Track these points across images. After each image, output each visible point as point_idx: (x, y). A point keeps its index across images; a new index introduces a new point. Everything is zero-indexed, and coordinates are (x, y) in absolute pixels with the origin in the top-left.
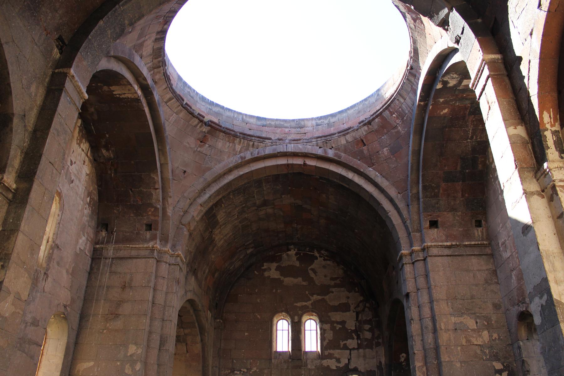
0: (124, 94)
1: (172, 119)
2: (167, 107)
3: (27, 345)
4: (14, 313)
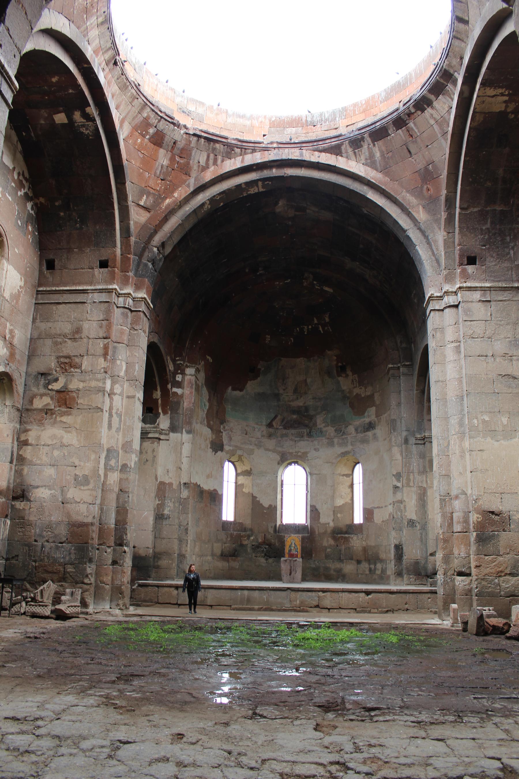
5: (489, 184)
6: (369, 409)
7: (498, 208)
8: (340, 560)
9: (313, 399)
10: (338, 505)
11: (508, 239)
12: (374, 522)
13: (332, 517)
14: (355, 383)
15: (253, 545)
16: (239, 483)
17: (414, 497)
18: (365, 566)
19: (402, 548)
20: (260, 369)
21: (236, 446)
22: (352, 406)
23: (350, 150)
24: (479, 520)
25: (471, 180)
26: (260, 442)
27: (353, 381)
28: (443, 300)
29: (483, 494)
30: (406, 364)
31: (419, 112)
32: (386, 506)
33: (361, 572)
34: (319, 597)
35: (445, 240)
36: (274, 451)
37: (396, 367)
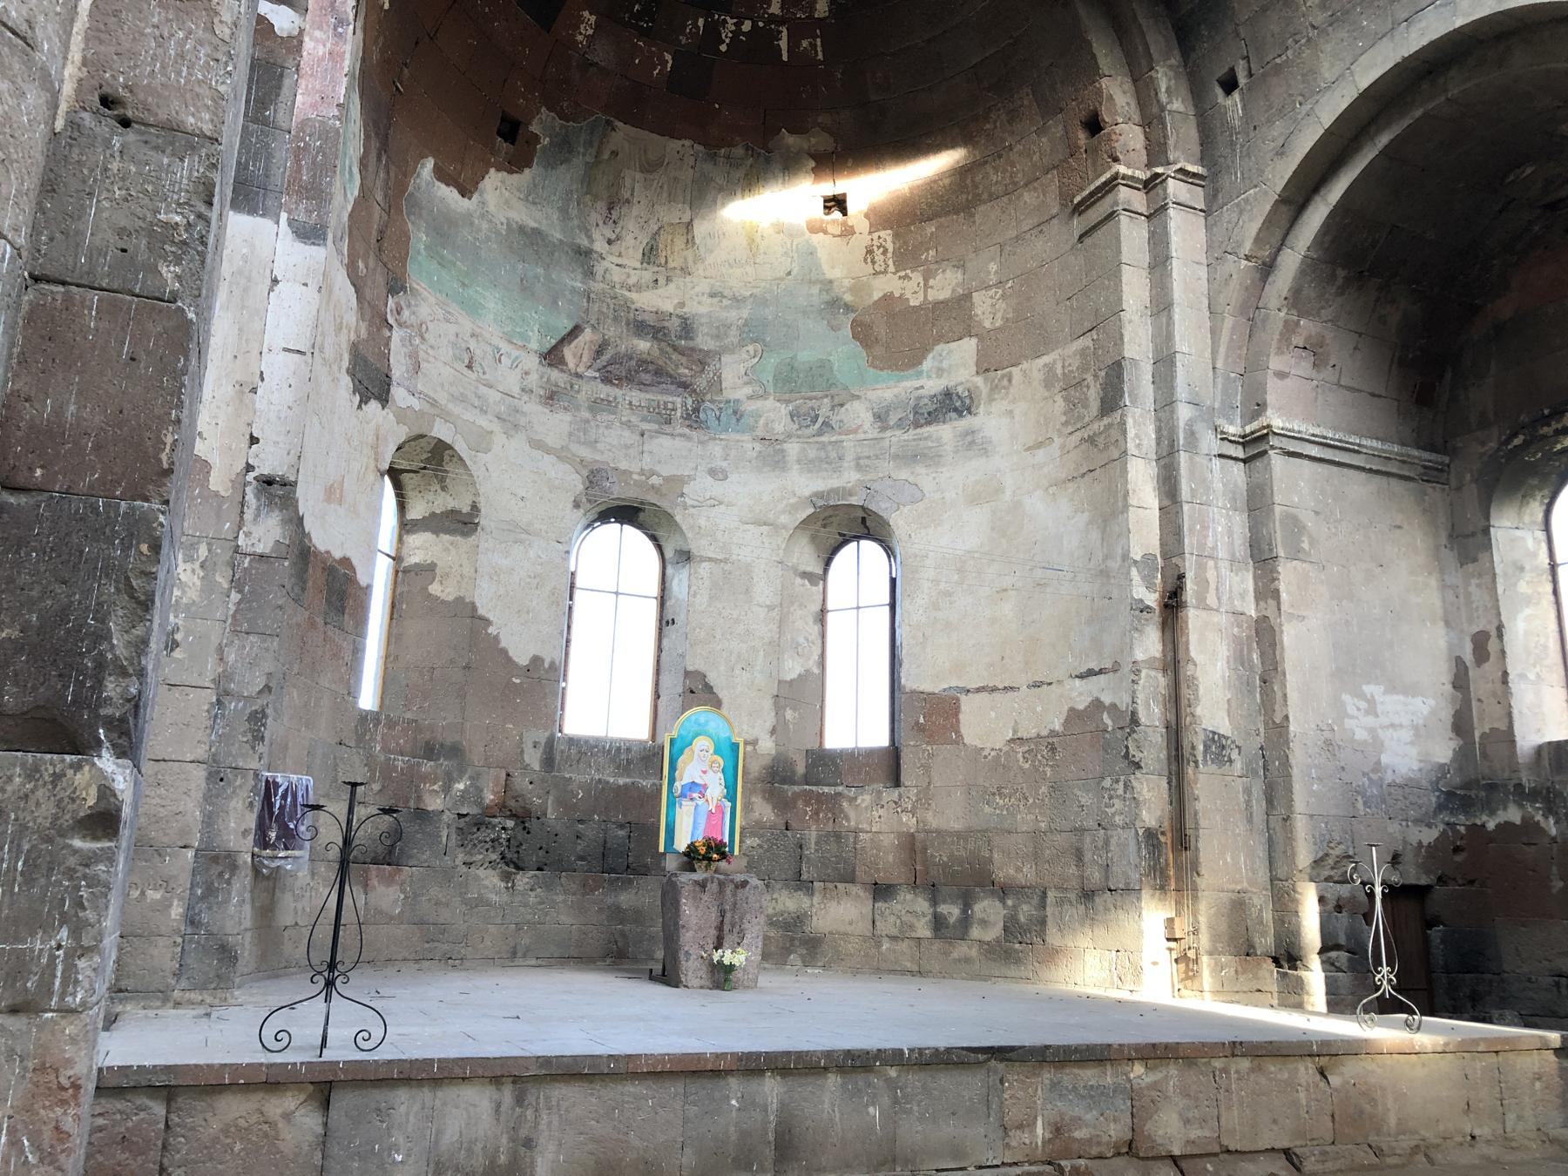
6: (938, 348)
8: (799, 883)
9: (712, 295)
10: (788, 679)
12: (959, 740)
13: (770, 720)
14: (879, 257)
15: (460, 816)
16: (413, 558)
17: (1223, 651)
18: (913, 908)
20: (536, 138)
21: (434, 403)
22: (863, 333)
26: (517, 411)
27: (870, 252)
32: (1037, 685)
33: (895, 932)
34: (1133, 1094)
36: (561, 455)
37: (1137, 180)
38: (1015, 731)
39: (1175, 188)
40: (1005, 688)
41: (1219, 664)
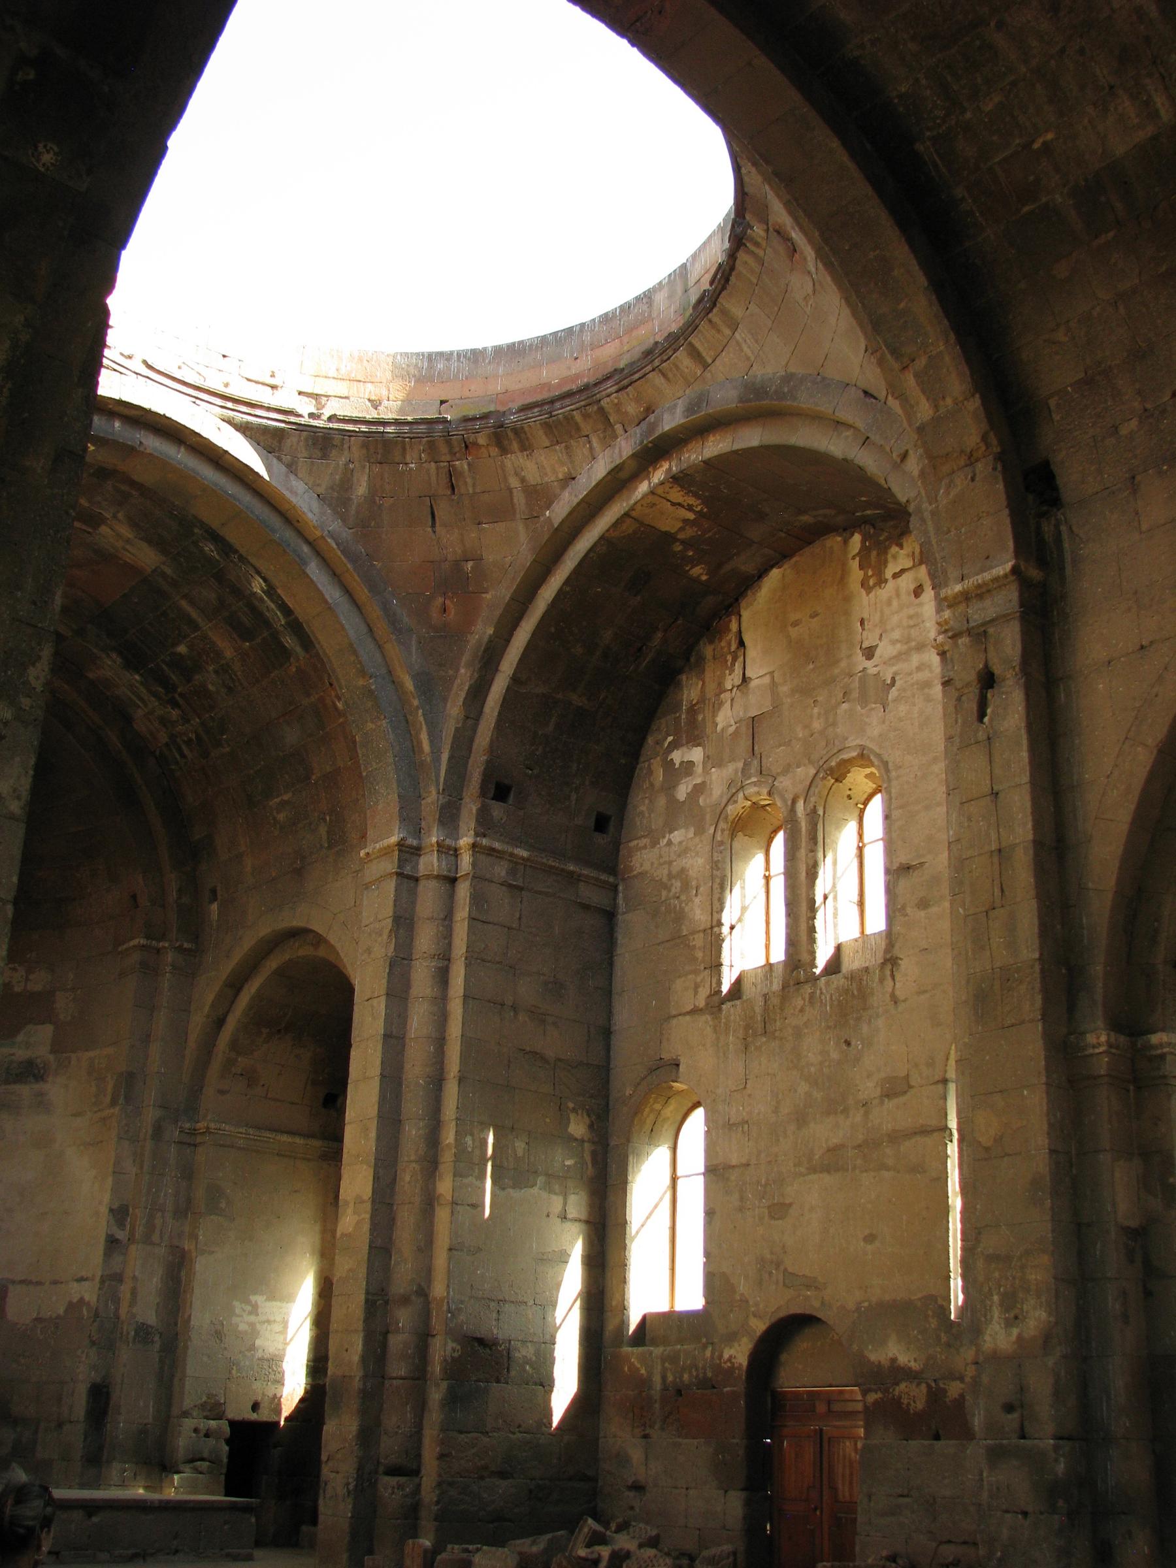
0: (673, 504)
1: (749, 347)
2: (717, 362)
3: (888, 1151)
4: (358, 1223)
5: (578, 650)
6: (29, 1027)
7: (577, 700)
11: (574, 767)
19: (108, 1393)
23: (303, 453)
24: (456, 1355)
25: (553, 630)
28: (420, 855)
29: (467, 1299)
30: (186, 945)
31: (494, 451)
32: (55, 1282)
35: (457, 729)
38: (38, 1313)
39: (170, 957)
40: (37, 1282)
41: (155, 1280)
